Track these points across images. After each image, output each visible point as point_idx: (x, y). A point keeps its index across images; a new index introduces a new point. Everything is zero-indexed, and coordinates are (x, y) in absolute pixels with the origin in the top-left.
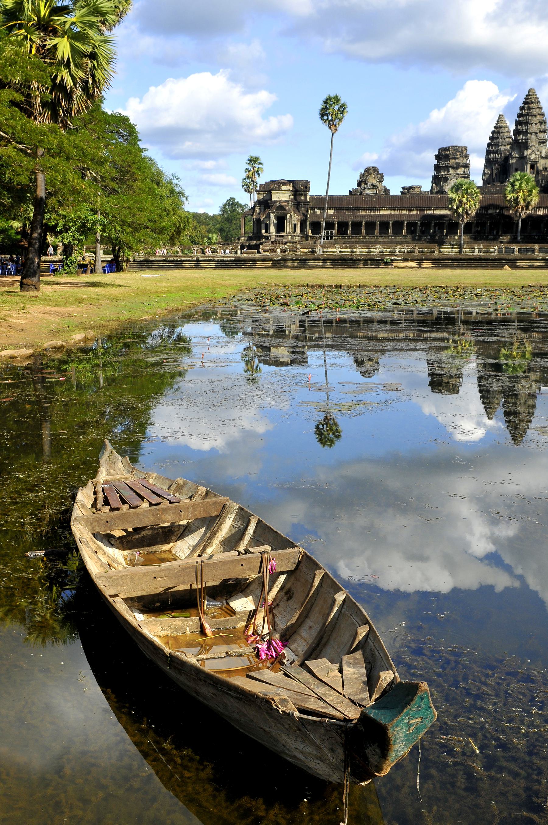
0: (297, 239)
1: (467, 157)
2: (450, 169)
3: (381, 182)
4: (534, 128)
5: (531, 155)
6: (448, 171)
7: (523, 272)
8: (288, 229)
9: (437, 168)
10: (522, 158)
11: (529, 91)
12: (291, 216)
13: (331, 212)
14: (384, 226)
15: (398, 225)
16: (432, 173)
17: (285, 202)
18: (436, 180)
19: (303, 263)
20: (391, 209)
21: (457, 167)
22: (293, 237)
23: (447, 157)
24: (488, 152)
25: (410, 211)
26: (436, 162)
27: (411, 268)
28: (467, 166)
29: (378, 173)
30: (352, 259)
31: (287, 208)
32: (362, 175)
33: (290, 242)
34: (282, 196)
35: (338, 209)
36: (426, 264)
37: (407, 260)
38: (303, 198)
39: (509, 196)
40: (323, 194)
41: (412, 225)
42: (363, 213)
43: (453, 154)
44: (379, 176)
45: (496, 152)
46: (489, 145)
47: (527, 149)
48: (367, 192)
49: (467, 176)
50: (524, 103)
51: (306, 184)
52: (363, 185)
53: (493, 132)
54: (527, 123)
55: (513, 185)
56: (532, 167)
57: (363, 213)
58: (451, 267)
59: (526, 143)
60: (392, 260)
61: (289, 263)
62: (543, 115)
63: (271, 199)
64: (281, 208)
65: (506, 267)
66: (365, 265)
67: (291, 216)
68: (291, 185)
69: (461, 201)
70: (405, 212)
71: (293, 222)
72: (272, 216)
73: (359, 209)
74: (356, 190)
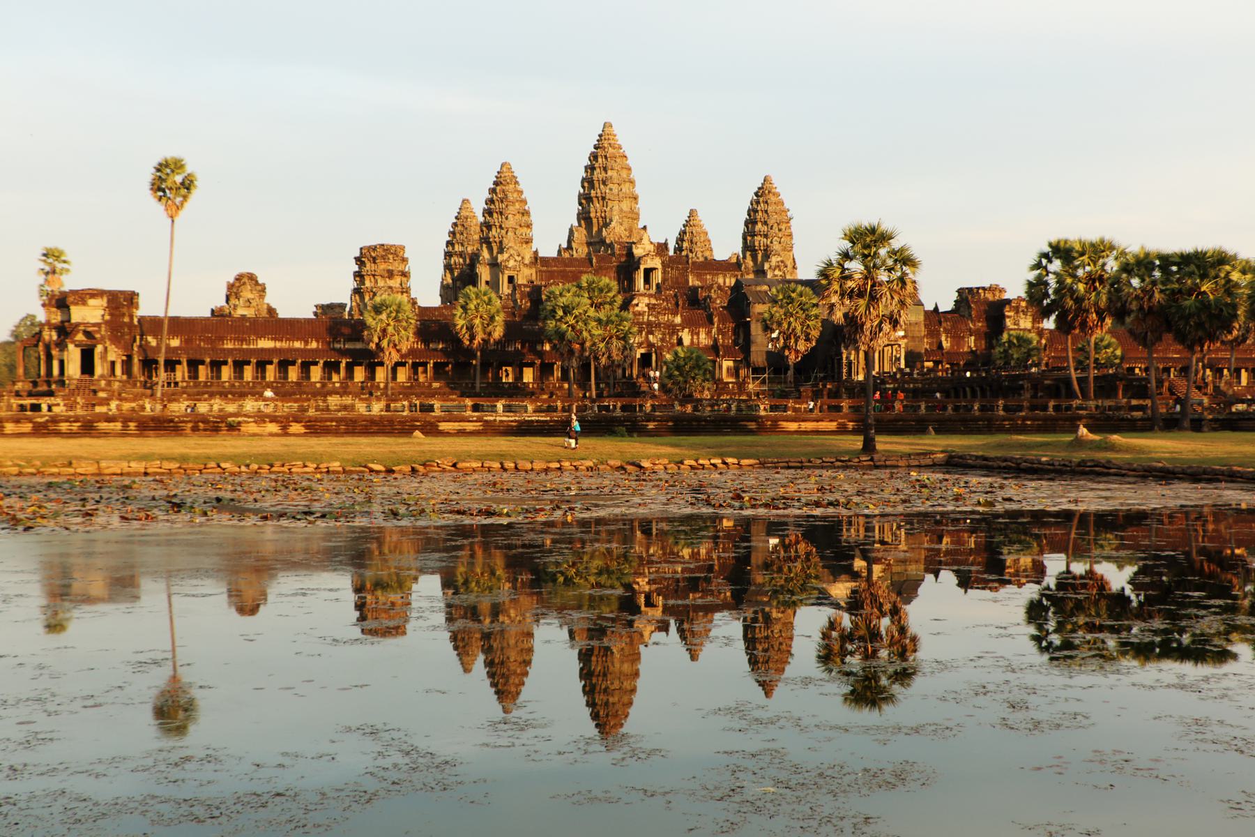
1: (404, 260)
2: (379, 279)
3: (262, 297)
4: (511, 222)
5: (508, 260)
6: (376, 282)
8: (99, 369)
9: (359, 276)
11: (502, 165)
12: (106, 349)
13: (175, 343)
16: (351, 284)
17: (94, 325)
18: (357, 291)
19: (88, 428)
20: (275, 339)
21: (391, 274)
22: (109, 383)
24: (448, 255)
25: (306, 343)
26: (356, 268)
27: (271, 435)
29: (257, 283)
30: (172, 421)
31: (98, 336)
32: (231, 287)
33: (103, 390)
34: (90, 314)
36: (296, 428)
38: (126, 320)
39: (460, 322)
40: (161, 314)
43: (383, 257)
45: (461, 255)
46: (448, 243)
47: (501, 250)
48: (240, 312)
49: (405, 291)
50: (496, 183)
51: (131, 298)
52: (233, 301)
55: (464, 308)
56: (511, 279)
58: (336, 433)
59: (501, 242)
60: (239, 423)
61: (64, 427)
62: (524, 202)
63: (69, 321)
65: (417, 433)
66: (195, 429)
67: (106, 349)
68: (105, 299)
69: (384, 331)
70: (297, 345)
71: (112, 356)
73: (222, 339)
74: (221, 309)
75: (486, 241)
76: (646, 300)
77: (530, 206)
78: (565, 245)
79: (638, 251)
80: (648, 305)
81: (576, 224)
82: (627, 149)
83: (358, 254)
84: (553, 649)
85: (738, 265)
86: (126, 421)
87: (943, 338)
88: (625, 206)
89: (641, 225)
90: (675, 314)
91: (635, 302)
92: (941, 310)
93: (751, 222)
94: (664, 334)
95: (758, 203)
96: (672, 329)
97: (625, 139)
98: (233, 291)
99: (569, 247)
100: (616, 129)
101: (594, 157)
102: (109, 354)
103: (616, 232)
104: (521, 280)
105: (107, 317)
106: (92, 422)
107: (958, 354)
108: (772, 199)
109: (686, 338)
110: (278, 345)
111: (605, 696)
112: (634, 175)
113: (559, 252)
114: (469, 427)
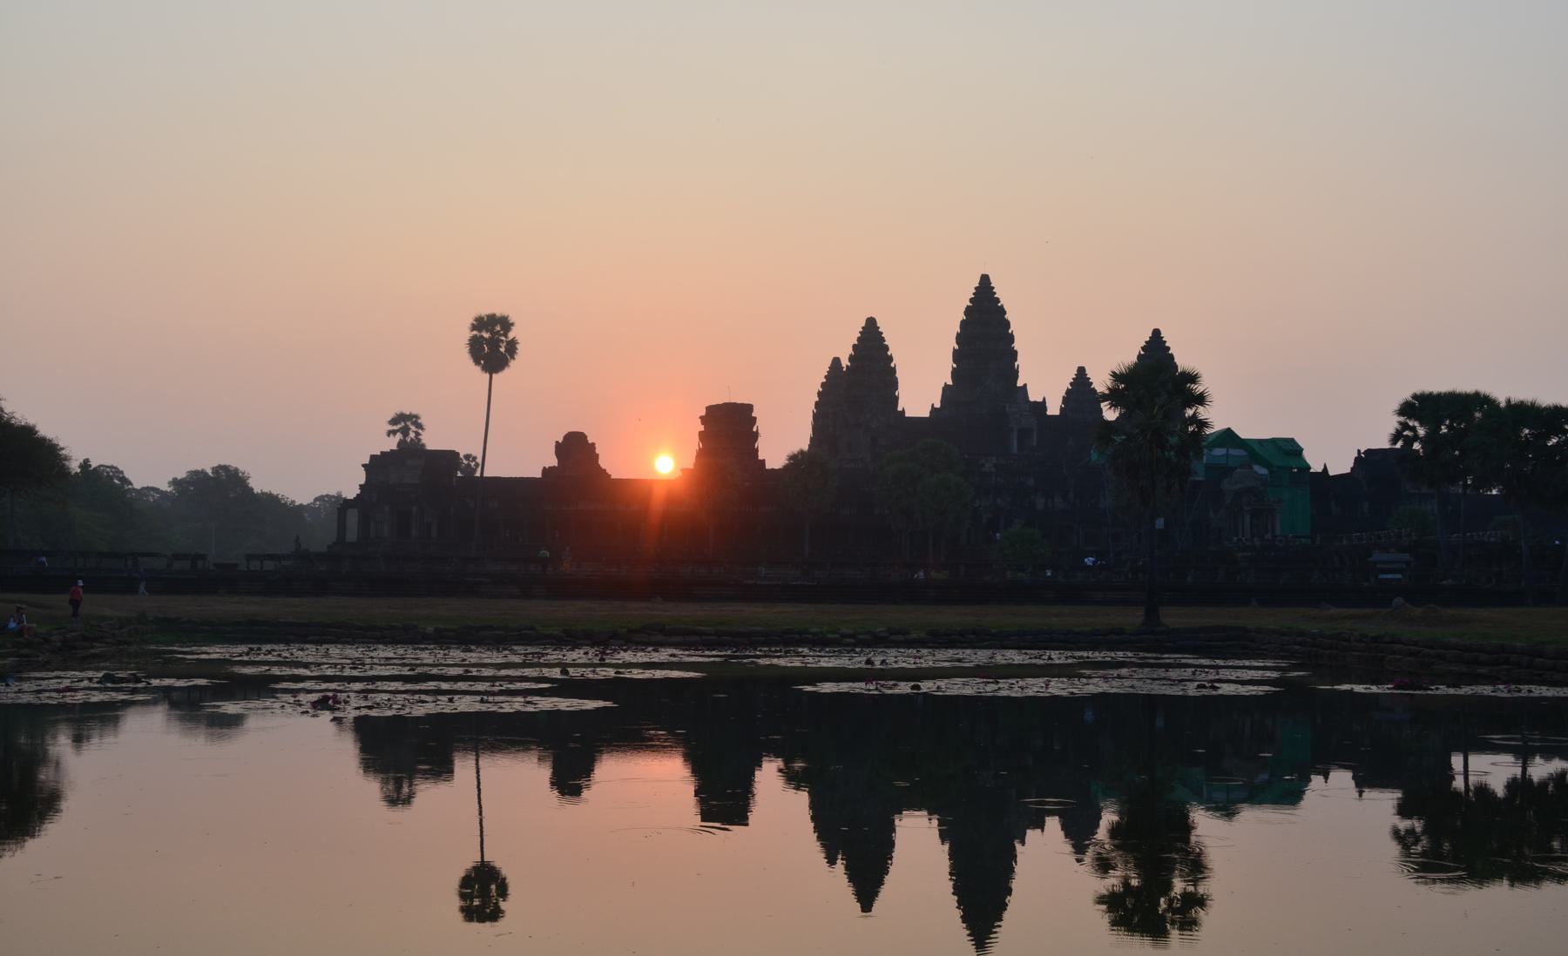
26: (702, 428)
78: (938, 405)
81: (950, 382)
82: (1004, 301)
83: (703, 413)
84: (918, 841)
89: (1020, 383)
92: (1331, 473)
97: (1004, 293)
101: (968, 311)
109: (1040, 503)
111: (982, 894)
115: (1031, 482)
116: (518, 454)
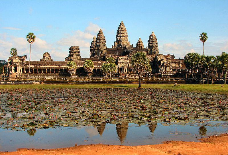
0: (21, 74)
4: (101, 41)
7: (70, 85)
8: (18, 71)
9: (70, 52)
10: (98, 50)
13: (32, 66)
14: (48, 70)
15: (53, 70)
16: (68, 54)
23: (73, 49)
24: (91, 47)
28: (79, 52)
34: (16, 61)
35: (34, 65)
36: (42, 83)
37: (37, 82)
41: (57, 71)
42: (42, 66)
44: (49, 55)
45: (93, 47)
46: (91, 45)
47: (100, 47)
48: (45, 60)
53: (92, 41)
54: (99, 40)
57: (42, 66)
61: (2, 83)
62: (104, 37)
64: (15, 65)
71: (20, 69)
72: (12, 67)
75: (96, 45)
76: (121, 57)
77: (106, 38)
79: (127, 46)
80: (122, 58)
85: (147, 49)
86: (12, 82)
87: (180, 65)
88: (125, 38)
90: (127, 60)
91: (119, 58)
93: (149, 41)
94: (125, 64)
95: (151, 37)
96: (127, 63)
98: (44, 56)
99: (114, 46)
100: (124, 22)
101: (119, 28)
102: (20, 69)
103: (123, 42)
104: (103, 53)
105: (19, 61)
106: (7, 82)
107: (183, 68)
108: (154, 36)
110: (51, 66)
112: (127, 31)
113: (112, 47)
114: (74, 83)
115: (128, 61)
116: (35, 56)
